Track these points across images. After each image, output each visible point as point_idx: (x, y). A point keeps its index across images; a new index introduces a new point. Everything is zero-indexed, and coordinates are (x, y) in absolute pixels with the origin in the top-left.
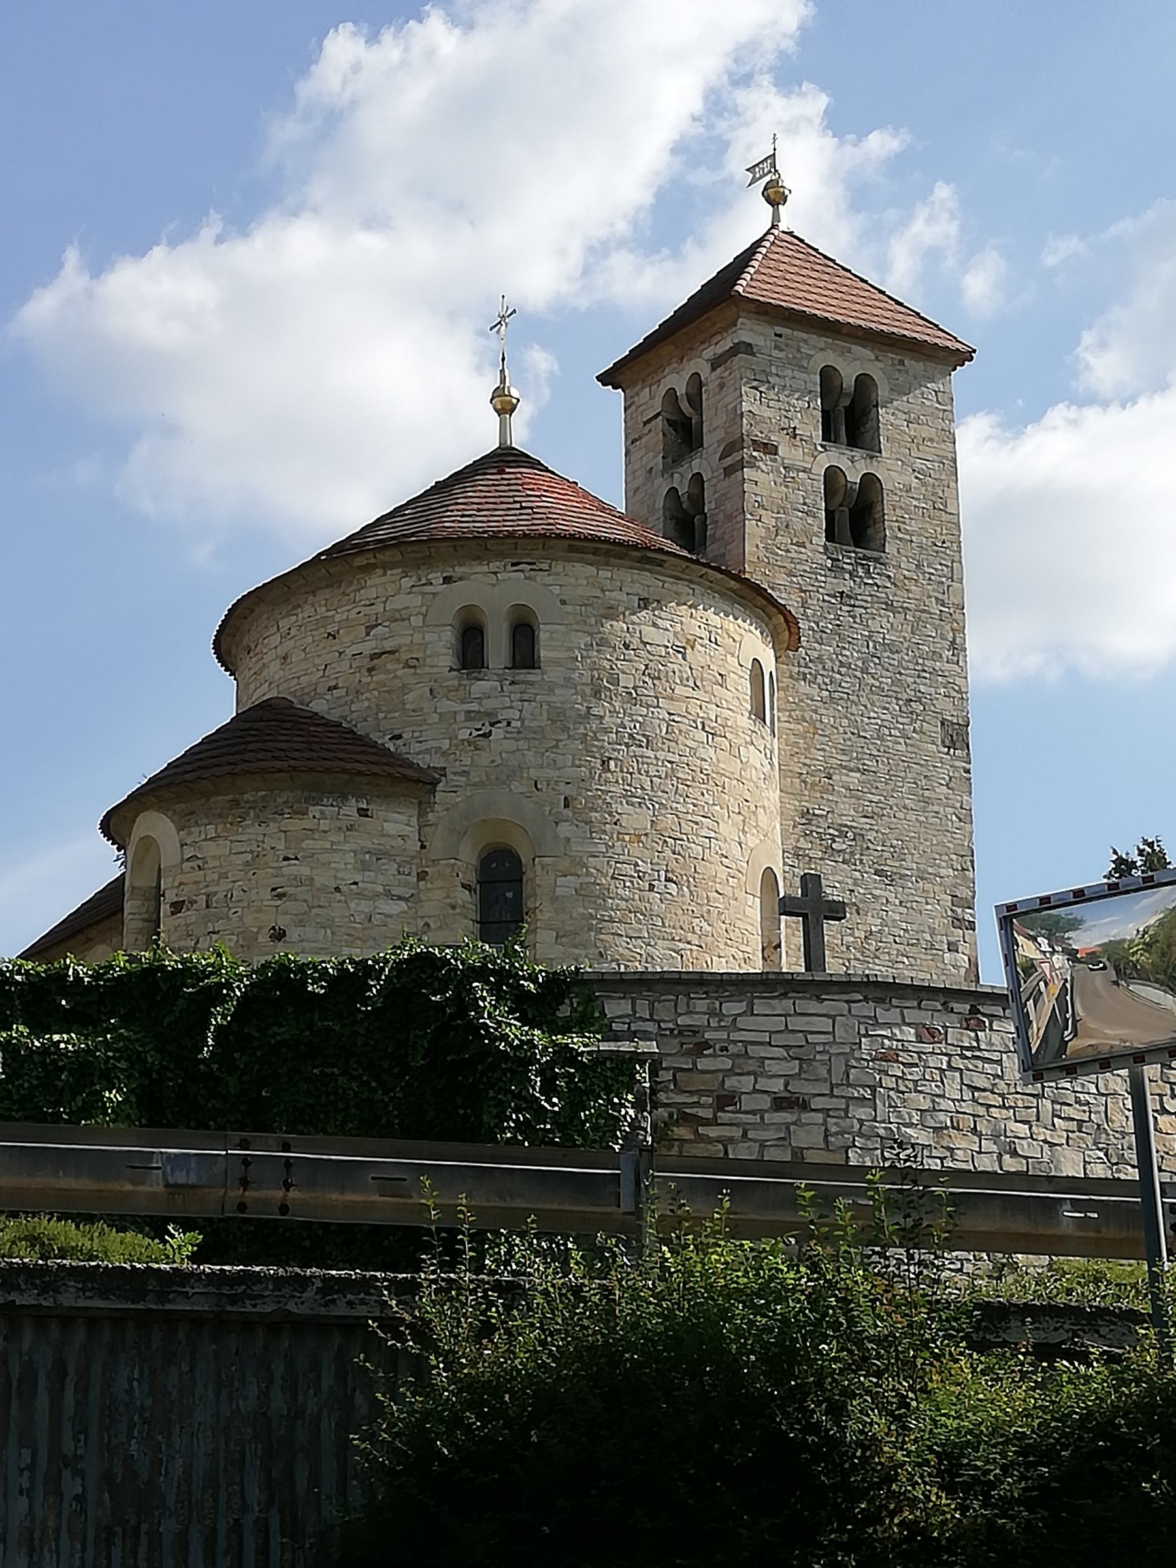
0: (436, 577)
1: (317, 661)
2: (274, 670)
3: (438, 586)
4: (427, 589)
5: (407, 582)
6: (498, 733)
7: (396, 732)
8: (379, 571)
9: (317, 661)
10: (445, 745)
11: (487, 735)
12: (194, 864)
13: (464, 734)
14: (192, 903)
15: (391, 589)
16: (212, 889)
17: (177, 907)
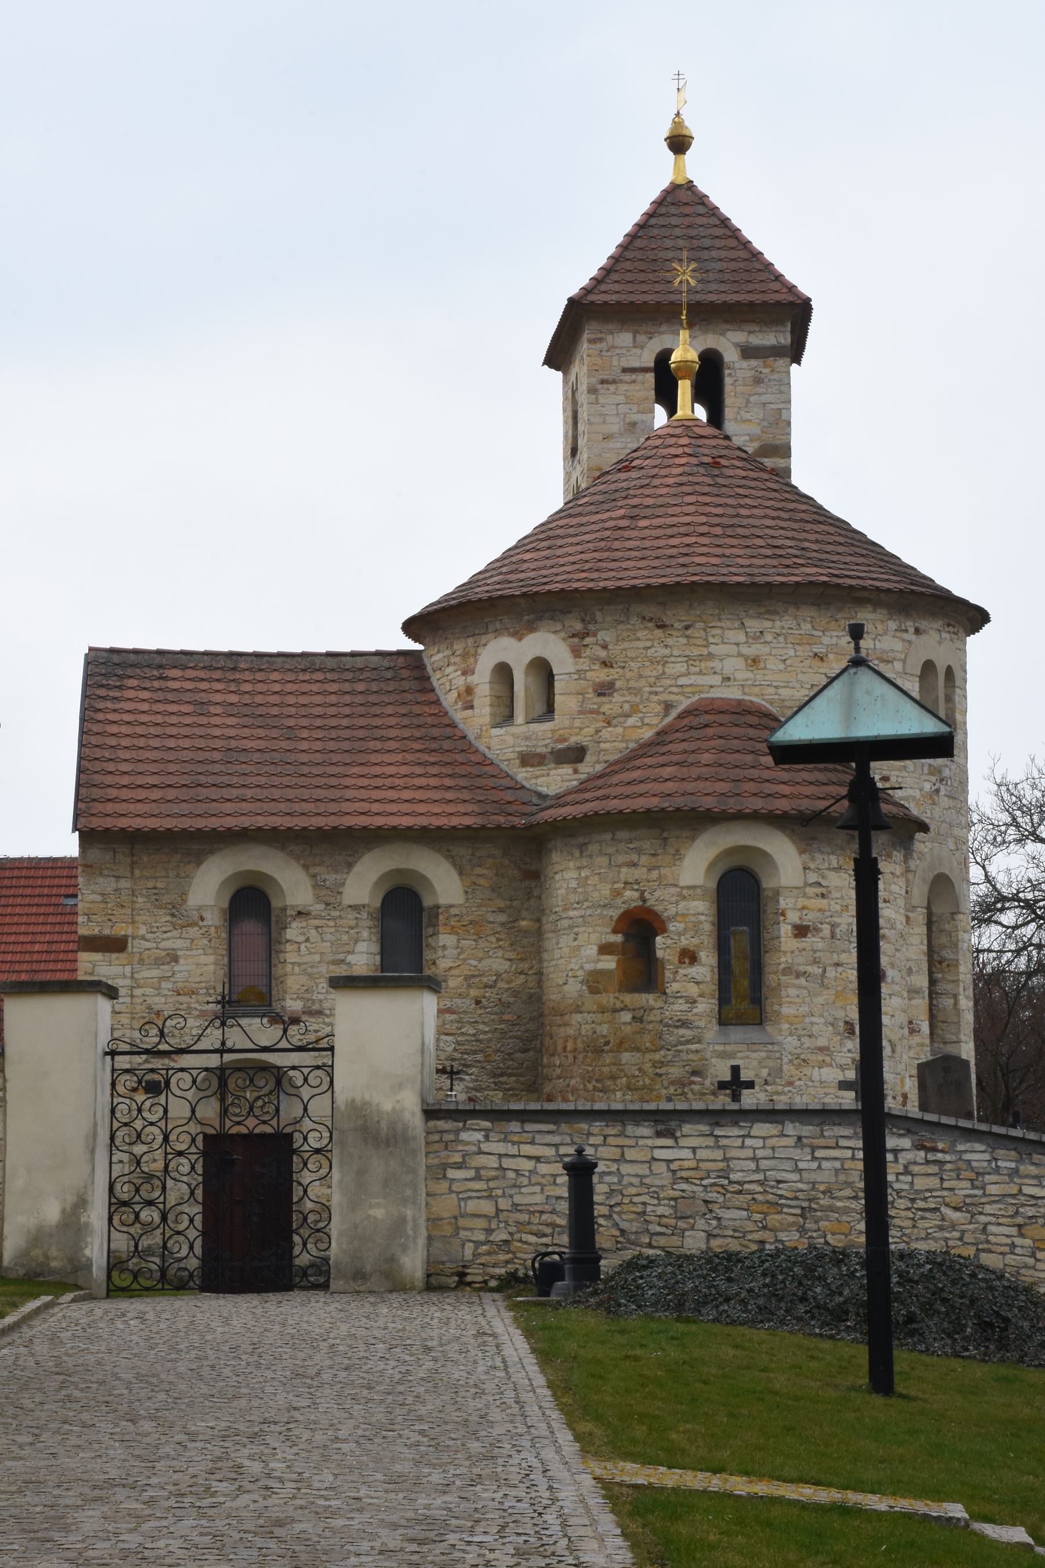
0: (910, 624)
1: (800, 677)
2: (734, 666)
3: (911, 636)
4: (905, 636)
5: (892, 625)
6: (942, 792)
7: (885, 773)
8: (870, 608)
9: (800, 677)
10: (917, 794)
11: (937, 791)
12: (819, 890)
13: (927, 787)
14: (817, 930)
15: (880, 627)
16: (837, 920)
17: (801, 931)
